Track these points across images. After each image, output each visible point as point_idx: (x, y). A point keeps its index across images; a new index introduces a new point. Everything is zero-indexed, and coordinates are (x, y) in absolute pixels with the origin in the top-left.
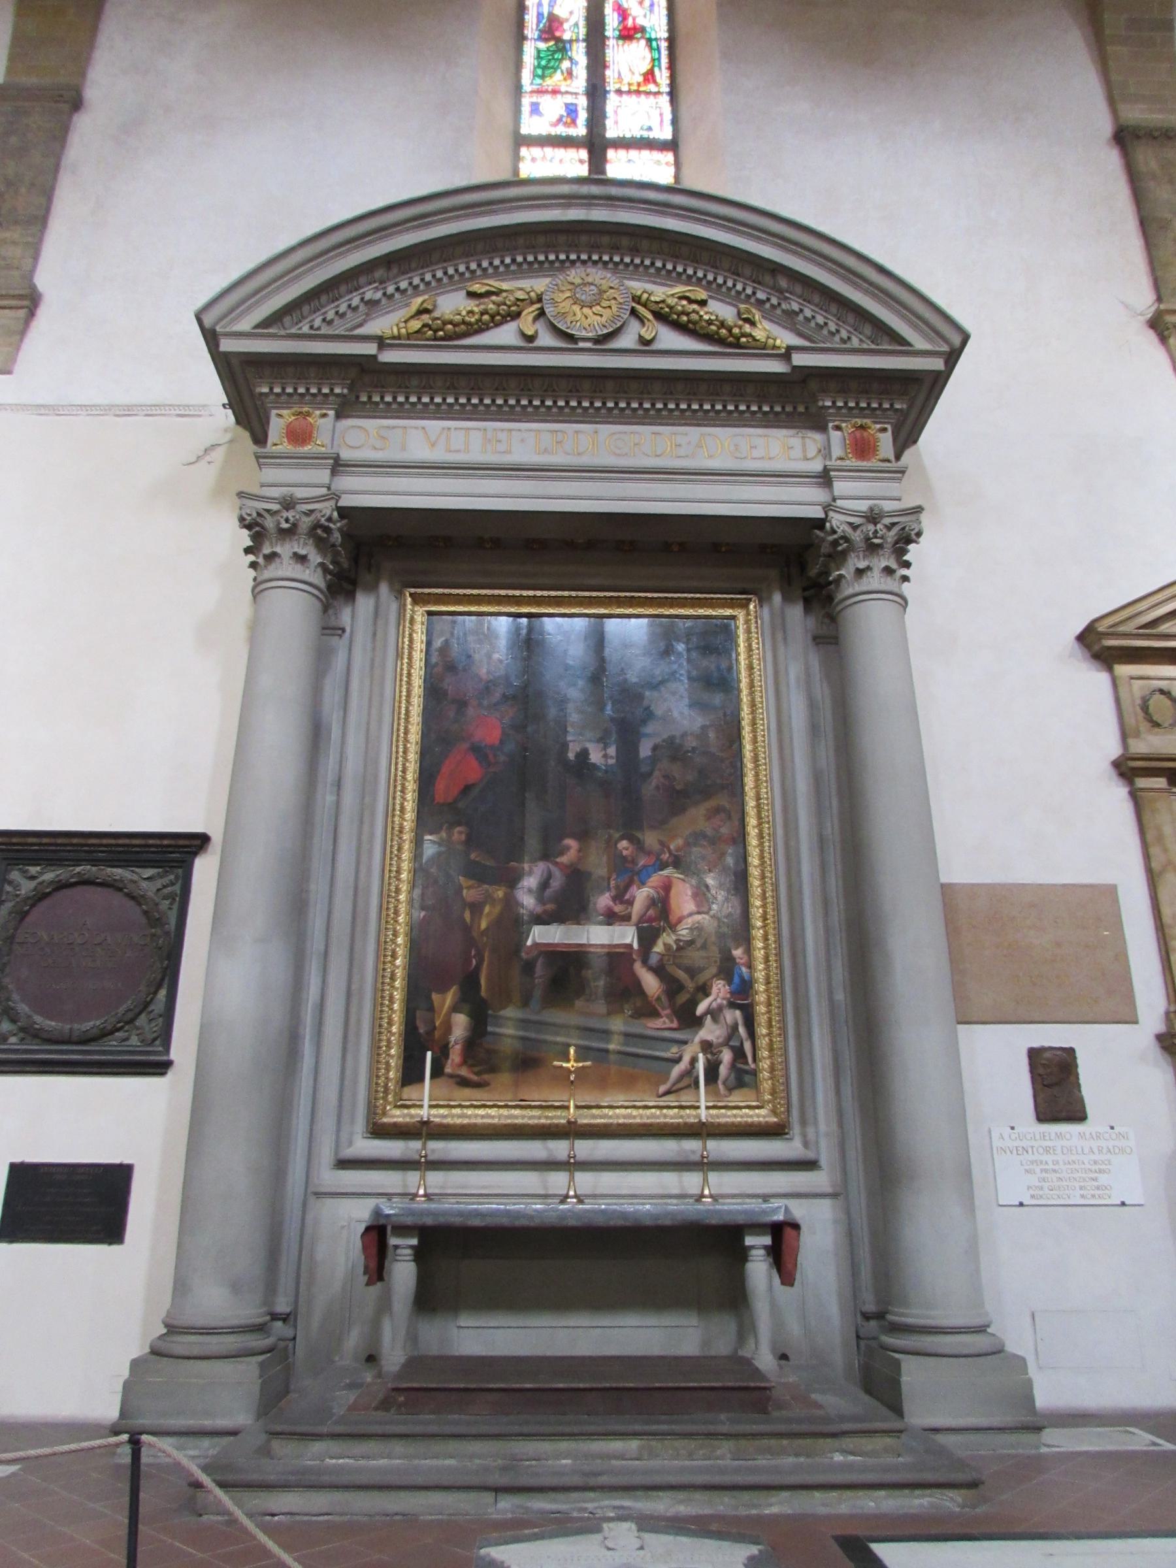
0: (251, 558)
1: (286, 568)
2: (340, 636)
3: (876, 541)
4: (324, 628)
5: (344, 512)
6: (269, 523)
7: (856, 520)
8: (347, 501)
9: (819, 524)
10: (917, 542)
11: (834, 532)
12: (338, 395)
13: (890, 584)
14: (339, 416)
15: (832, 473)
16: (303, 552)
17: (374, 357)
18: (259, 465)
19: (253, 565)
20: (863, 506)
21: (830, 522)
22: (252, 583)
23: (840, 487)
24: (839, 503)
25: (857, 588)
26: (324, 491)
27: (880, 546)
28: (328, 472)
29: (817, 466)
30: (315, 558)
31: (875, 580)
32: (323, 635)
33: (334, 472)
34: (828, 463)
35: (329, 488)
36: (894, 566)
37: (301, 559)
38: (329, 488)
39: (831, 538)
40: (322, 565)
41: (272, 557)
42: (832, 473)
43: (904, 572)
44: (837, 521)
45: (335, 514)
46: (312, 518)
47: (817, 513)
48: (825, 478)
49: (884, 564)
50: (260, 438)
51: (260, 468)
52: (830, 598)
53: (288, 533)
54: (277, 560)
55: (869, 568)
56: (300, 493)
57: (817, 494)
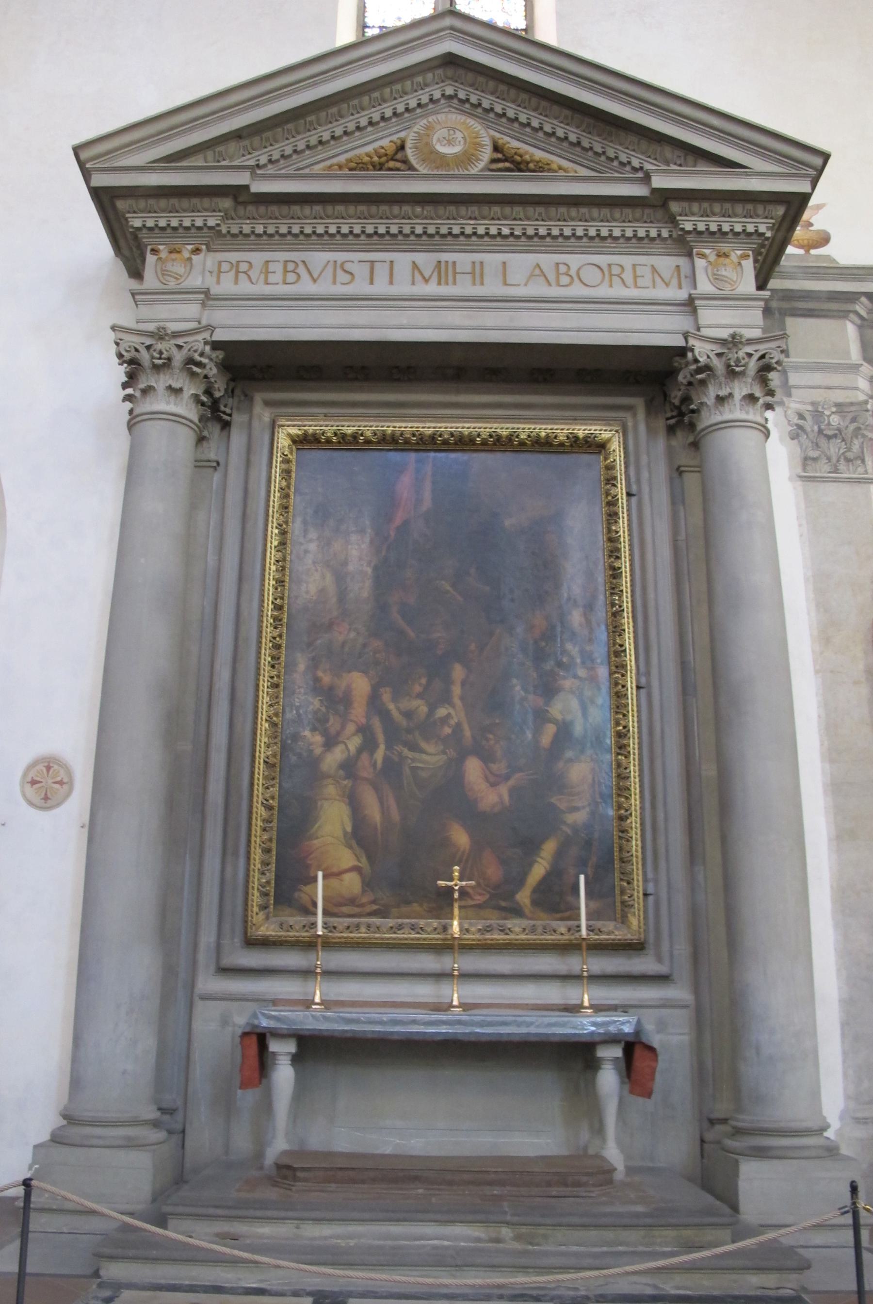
0: (130, 391)
1: (162, 403)
2: (215, 468)
3: (737, 369)
5: (216, 345)
6: (145, 357)
8: (220, 335)
9: (682, 352)
11: (696, 361)
12: (211, 228)
13: (752, 414)
16: (176, 385)
18: (135, 302)
19: (128, 398)
21: (692, 350)
22: (128, 417)
24: (705, 332)
25: (719, 418)
27: (743, 373)
30: (191, 389)
31: (735, 411)
32: (196, 467)
34: (693, 292)
35: (199, 323)
36: (758, 394)
40: (196, 398)
41: (147, 391)
43: (769, 399)
45: (208, 348)
47: (679, 342)
48: (690, 305)
49: (746, 391)
50: (136, 273)
51: (137, 305)
52: (692, 426)
53: (164, 366)
55: (731, 395)
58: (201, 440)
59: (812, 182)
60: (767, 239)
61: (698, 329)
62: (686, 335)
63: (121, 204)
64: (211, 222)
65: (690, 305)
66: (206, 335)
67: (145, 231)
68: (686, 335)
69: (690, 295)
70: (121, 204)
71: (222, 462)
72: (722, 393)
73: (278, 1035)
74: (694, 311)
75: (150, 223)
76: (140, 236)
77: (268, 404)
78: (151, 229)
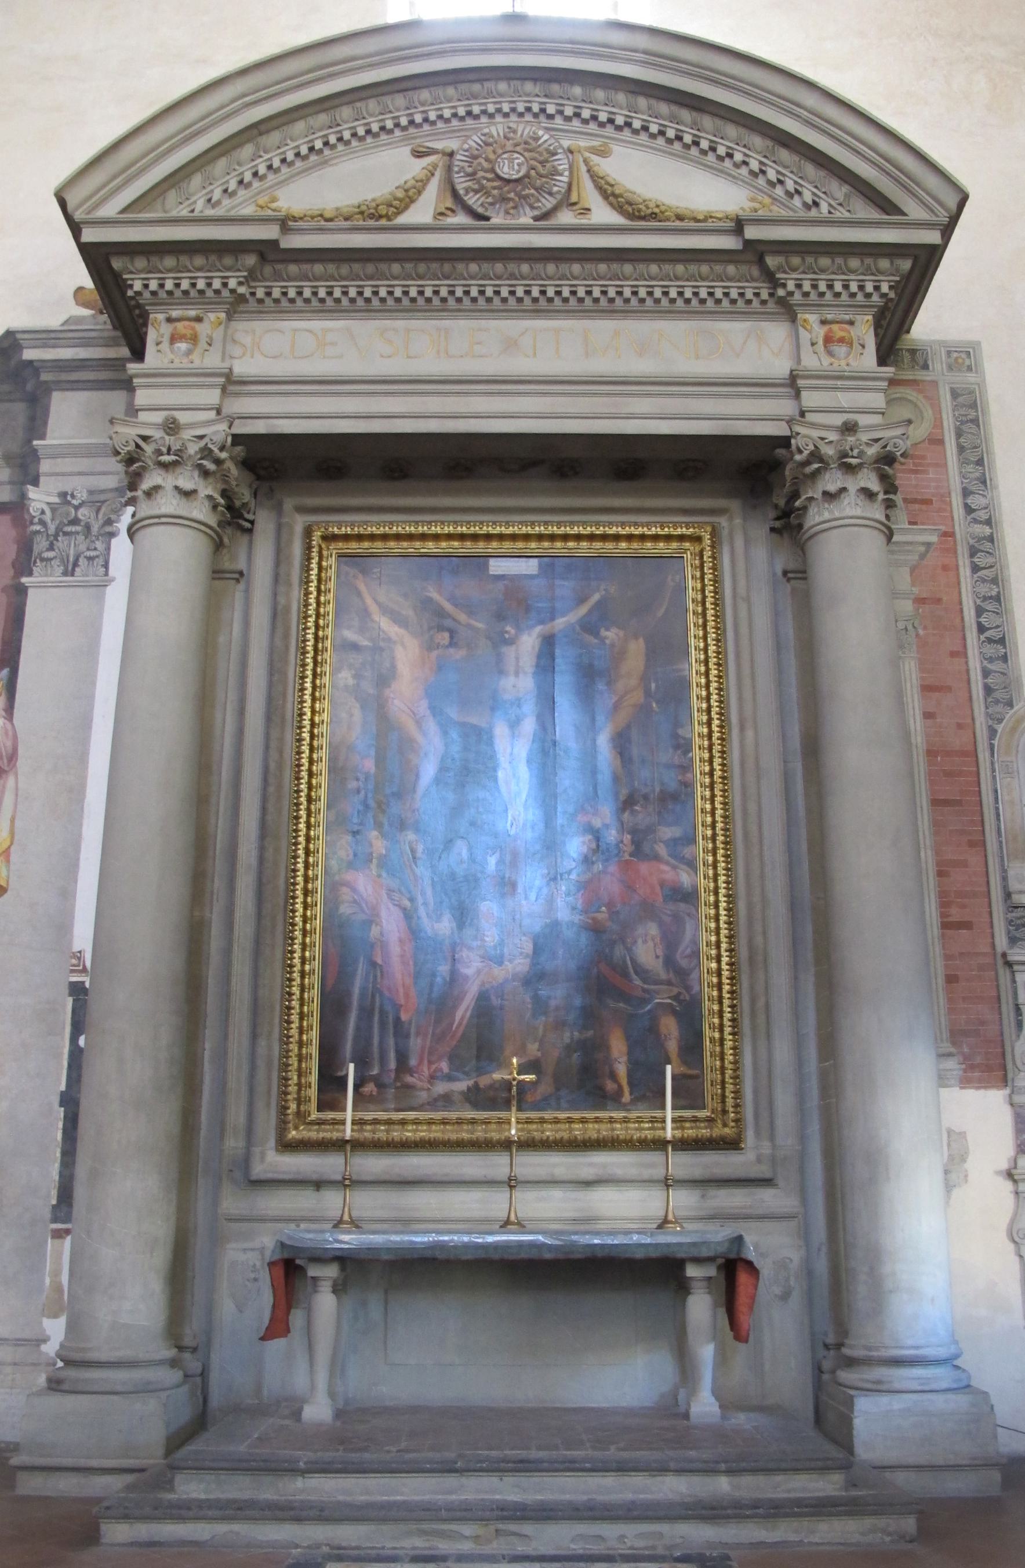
2: (238, 581)
4: (214, 572)
9: (784, 442)
20: (838, 420)
23: (810, 399)
24: (810, 417)
30: (207, 489)
32: (214, 579)
37: (188, 494)
39: (798, 457)
40: (210, 497)
44: (806, 437)
46: (202, 444)
54: (160, 492)
55: (844, 490)
57: (786, 407)
58: (218, 546)
60: (891, 300)
61: (802, 414)
62: (790, 422)
65: (793, 383)
68: (790, 422)
71: (245, 572)
72: (832, 488)
73: (320, 1258)
74: (797, 395)
77: (301, 510)
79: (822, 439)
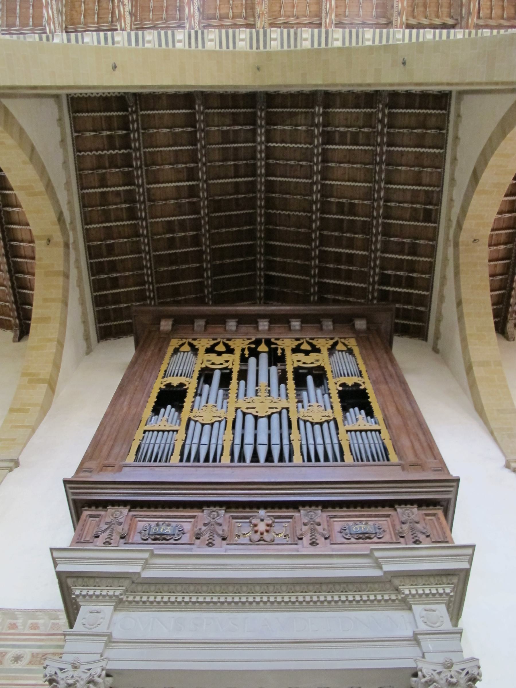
7: (439, 669)
10: (480, 680)
11: (424, 676)
14: (115, 610)
15: (420, 637)
17: (139, 574)
26: (98, 657)
28: (103, 645)
29: (409, 633)
33: (106, 646)
38: (101, 656)
39: (423, 680)
42: (420, 637)
45: (104, 673)
47: (410, 664)
56: (83, 658)
57: (413, 651)
59: (468, 562)
63: (70, 581)
64: (117, 593)
66: (103, 664)
67: (81, 597)
69: (414, 632)
70: (70, 581)
74: (418, 644)
75: (84, 593)
76: (78, 600)
78: (84, 596)
79: (435, 670)
